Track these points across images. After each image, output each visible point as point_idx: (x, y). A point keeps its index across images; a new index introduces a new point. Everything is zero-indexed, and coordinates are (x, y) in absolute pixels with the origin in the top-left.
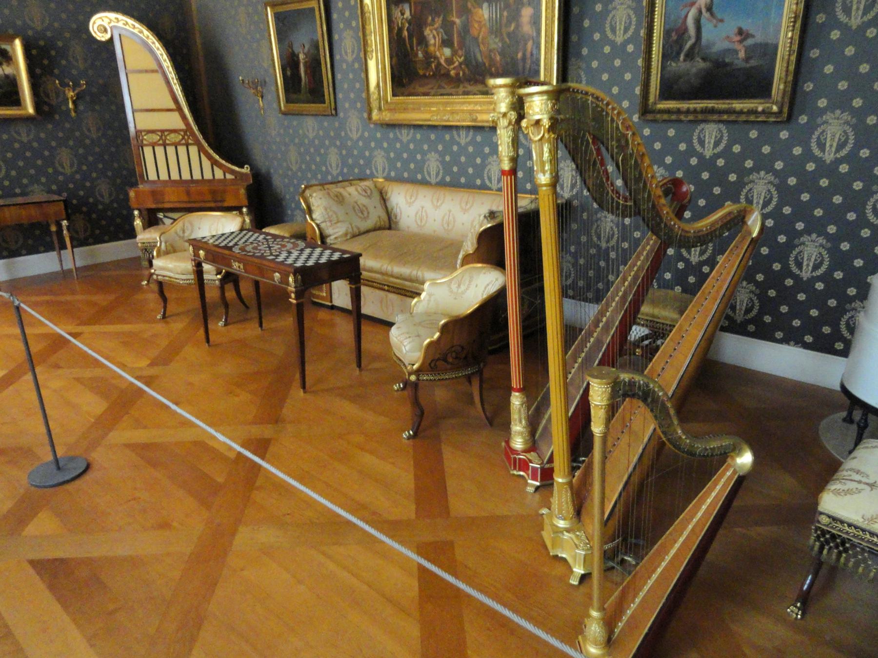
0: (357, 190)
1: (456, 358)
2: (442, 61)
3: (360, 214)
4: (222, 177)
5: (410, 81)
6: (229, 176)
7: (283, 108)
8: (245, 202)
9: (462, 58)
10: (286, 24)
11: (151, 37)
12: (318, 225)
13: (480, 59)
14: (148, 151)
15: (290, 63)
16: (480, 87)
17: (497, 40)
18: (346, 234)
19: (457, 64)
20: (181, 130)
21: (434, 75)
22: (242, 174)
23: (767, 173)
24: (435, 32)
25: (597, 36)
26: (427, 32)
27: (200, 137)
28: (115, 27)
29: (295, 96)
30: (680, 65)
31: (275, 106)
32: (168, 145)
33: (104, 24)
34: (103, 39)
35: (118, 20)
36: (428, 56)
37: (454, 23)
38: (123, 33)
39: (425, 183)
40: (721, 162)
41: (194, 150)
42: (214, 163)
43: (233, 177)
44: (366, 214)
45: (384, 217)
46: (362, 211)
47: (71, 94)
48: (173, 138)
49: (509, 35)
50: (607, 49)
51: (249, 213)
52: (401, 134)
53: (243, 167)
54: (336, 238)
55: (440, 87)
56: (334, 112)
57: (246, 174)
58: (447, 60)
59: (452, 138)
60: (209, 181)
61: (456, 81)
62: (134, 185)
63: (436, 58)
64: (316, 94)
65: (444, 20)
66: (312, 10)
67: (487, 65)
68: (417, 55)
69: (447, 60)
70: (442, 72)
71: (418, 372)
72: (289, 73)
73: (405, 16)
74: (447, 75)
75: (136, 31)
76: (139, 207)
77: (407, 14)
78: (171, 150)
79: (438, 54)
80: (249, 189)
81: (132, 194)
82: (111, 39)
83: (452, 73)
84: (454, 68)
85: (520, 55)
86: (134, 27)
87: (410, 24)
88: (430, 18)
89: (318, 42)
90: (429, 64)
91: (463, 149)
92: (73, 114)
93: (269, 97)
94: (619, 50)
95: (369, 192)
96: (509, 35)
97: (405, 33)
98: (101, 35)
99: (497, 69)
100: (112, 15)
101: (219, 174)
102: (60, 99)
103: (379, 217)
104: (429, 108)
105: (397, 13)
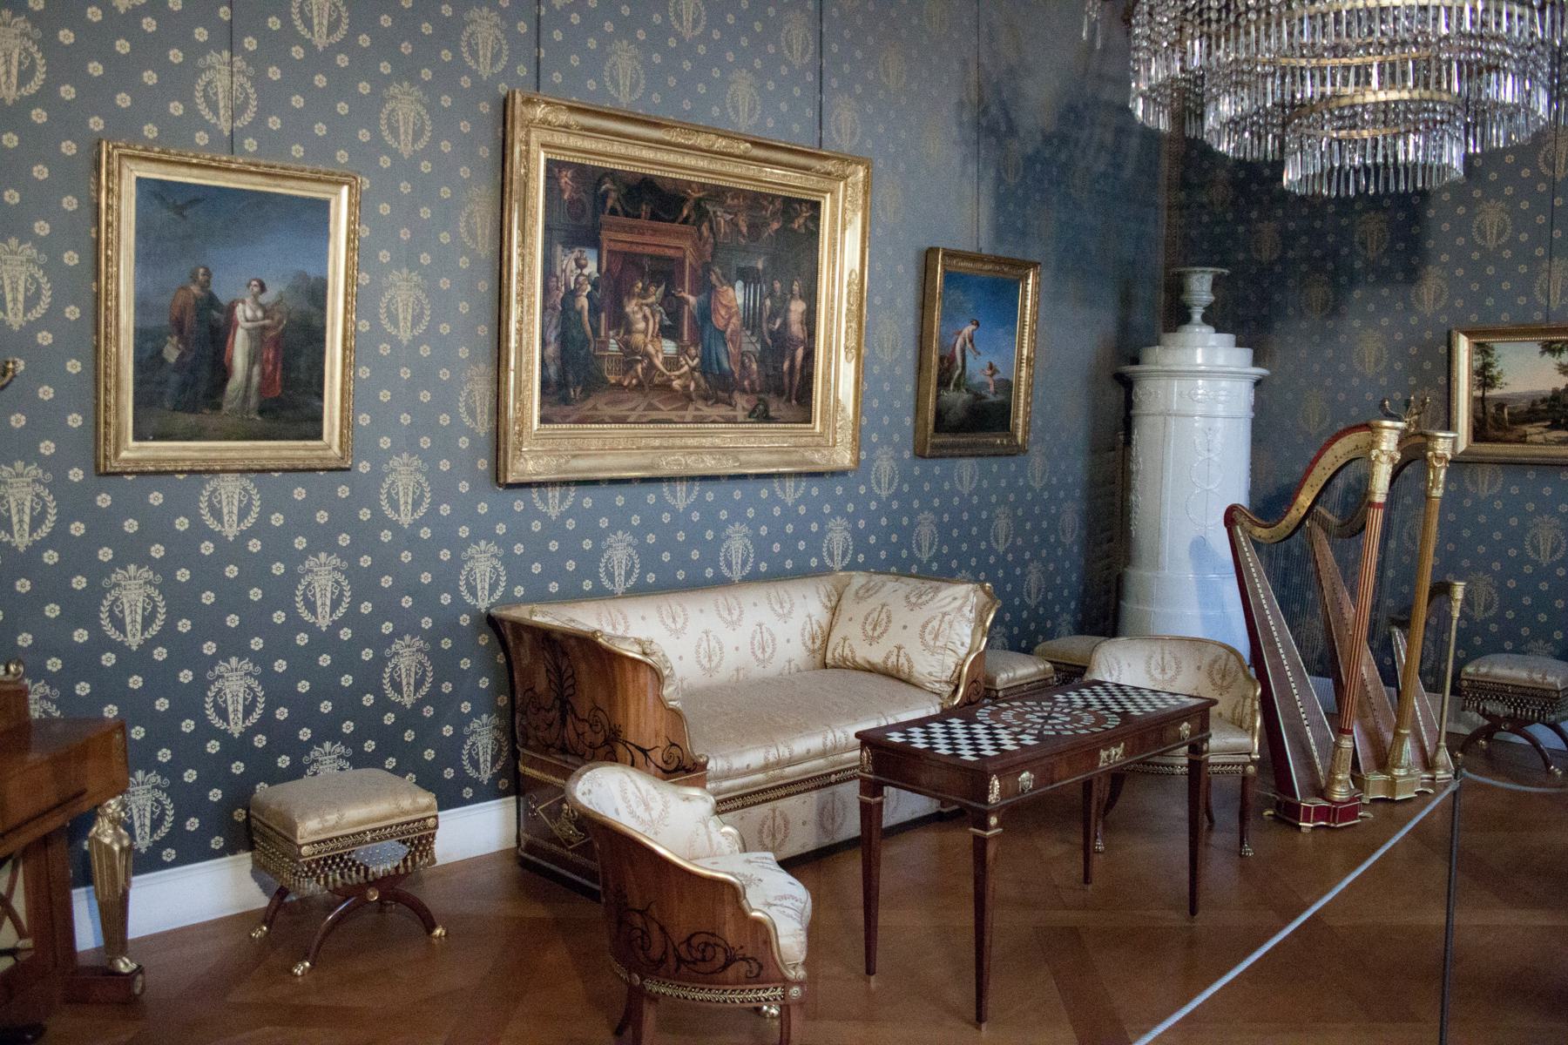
2: (658, 362)
5: (588, 391)
9: (696, 361)
13: (726, 365)
16: (723, 410)
17: (754, 339)
19: (686, 368)
21: (640, 385)
23: (140, 567)
24: (647, 311)
26: (631, 307)
30: (950, 395)
36: (631, 354)
37: (687, 302)
39: (721, 582)
40: (255, 546)
52: (545, 501)
55: (651, 407)
58: (666, 361)
59: (660, 498)
61: (686, 398)
63: (647, 355)
65: (667, 294)
68: (605, 344)
69: (666, 361)
70: (657, 380)
73: (586, 271)
74: (666, 386)
77: (591, 268)
79: (650, 348)
83: (676, 384)
84: (679, 377)
85: (786, 365)
87: (595, 285)
90: (629, 365)
91: (681, 519)
96: (771, 333)
97: (583, 302)
99: (752, 383)
104: (612, 446)
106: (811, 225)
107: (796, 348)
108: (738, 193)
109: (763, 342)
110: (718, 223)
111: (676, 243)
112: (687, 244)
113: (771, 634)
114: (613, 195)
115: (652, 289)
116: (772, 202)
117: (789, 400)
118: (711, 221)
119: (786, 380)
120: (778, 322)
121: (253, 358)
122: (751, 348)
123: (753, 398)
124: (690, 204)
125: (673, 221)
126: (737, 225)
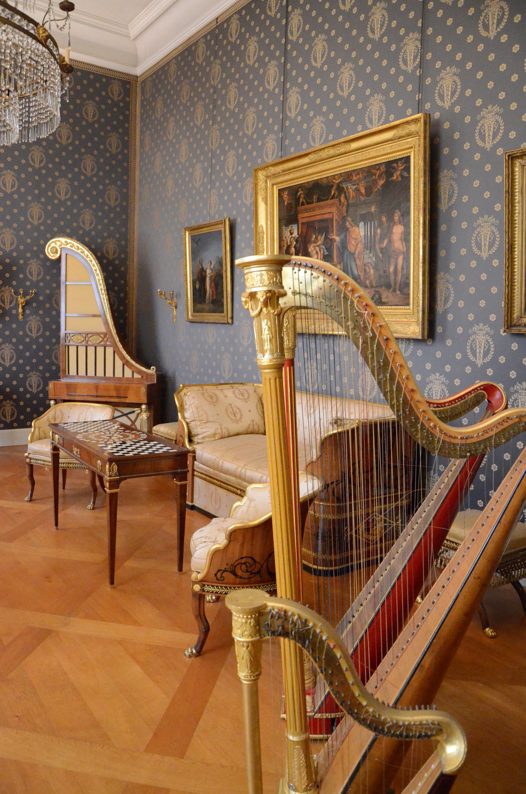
0: (234, 393)
1: (247, 571)
3: (232, 416)
4: (131, 376)
6: (136, 376)
7: (190, 317)
8: (144, 399)
10: (200, 242)
11: (90, 256)
12: (187, 424)
14: (72, 351)
15: (200, 278)
17: (371, 255)
18: (215, 435)
20: (102, 333)
22: (147, 374)
24: (317, 248)
25: (463, 252)
27: (117, 339)
28: (64, 248)
29: (199, 306)
31: (185, 315)
32: (90, 346)
33: (58, 246)
34: (53, 258)
35: (67, 243)
37: (333, 241)
38: (69, 253)
41: (110, 351)
42: (126, 363)
43: (140, 377)
44: (238, 417)
45: (261, 423)
46: (234, 414)
47: (21, 300)
48: (96, 340)
49: (382, 249)
50: (473, 264)
51: (149, 408)
53: (149, 368)
54: (203, 437)
56: (230, 321)
57: (151, 375)
60: (119, 379)
62: (56, 376)
64: (217, 305)
65: (326, 238)
66: (220, 232)
67: (362, 278)
71: (202, 582)
72: (197, 287)
73: (293, 236)
75: (79, 251)
76: (56, 397)
77: (295, 234)
78: (91, 350)
80: (150, 387)
81: (51, 385)
82: (59, 260)
85: (392, 269)
86: (78, 248)
87: (297, 241)
88: (314, 237)
89: (222, 258)
92: (20, 317)
93: (181, 307)
94: (484, 265)
95: (246, 396)
96: (382, 249)
98: (52, 255)
99: (371, 282)
100: (63, 240)
101: (128, 373)
102: (12, 305)
103: (253, 421)
105: (286, 233)
106: (405, 174)
107: (398, 255)
108: (357, 172)
109: (377, 257)
110: (349, 193)
111: (329, 210)
112: (334, 210)
113: (238, 409)
114: (302, 196)
115: (319, 237)
116: (379, 169)
117: (394, 291)
118: (345, 193)
119: (392, 278)
120: (386, 242)
121: (210, 285)
122: (369, 261)
123: (372, 291)
124: (334, 188)
125: (327, 200)
126: (359, 190)
